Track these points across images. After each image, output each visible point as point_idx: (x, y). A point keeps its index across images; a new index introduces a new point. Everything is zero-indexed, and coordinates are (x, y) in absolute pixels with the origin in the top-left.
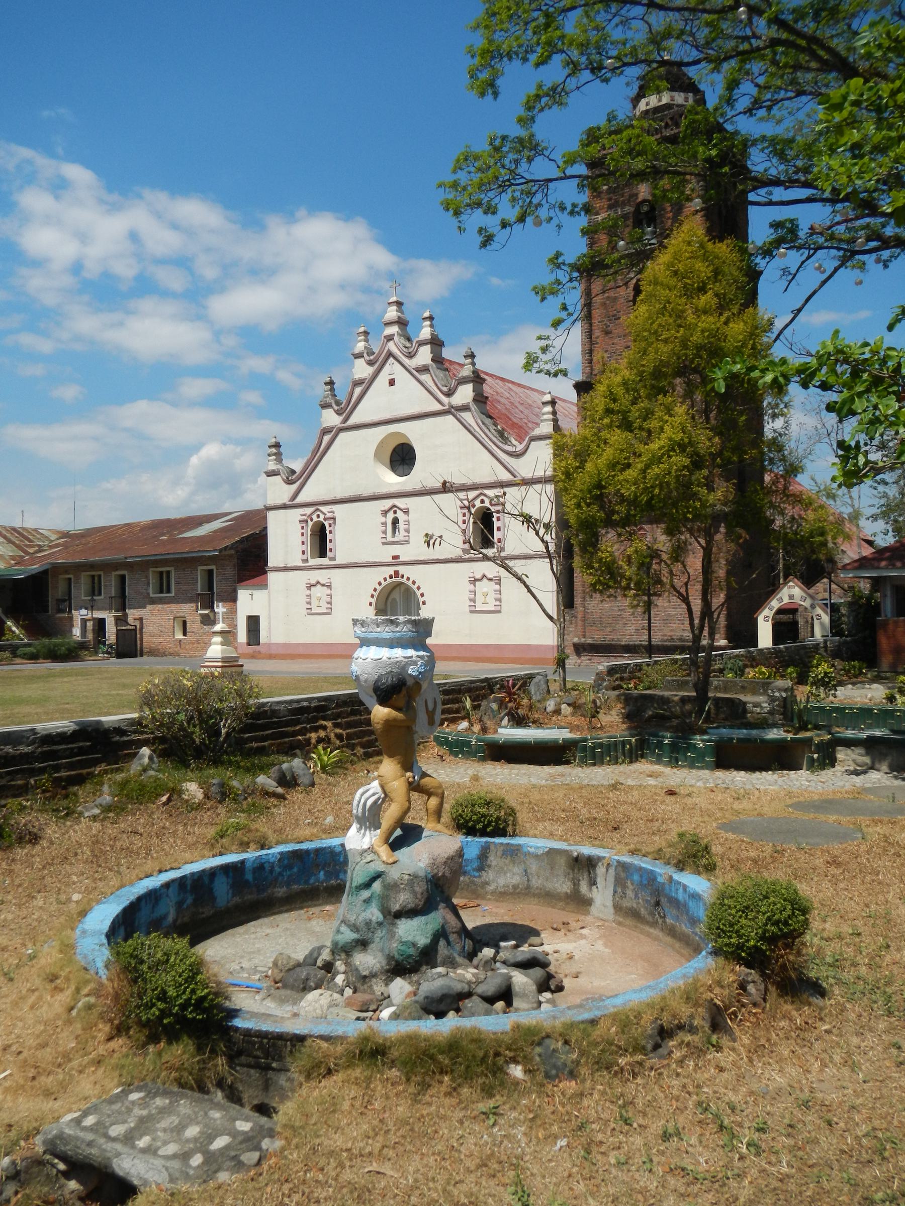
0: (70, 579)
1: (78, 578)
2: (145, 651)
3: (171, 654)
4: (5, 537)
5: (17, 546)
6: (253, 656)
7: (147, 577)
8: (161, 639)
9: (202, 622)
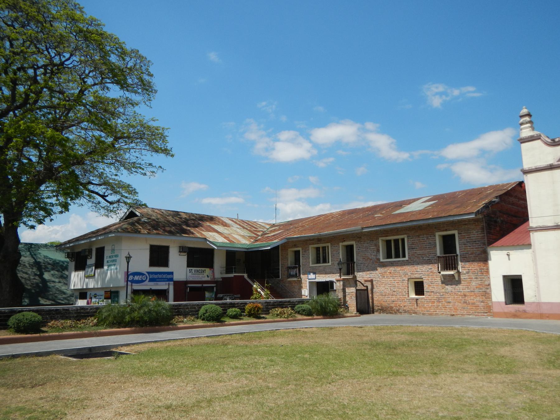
0: (299, 251)
1: (306, 250)
2: (376, 308)
3: (405, 312)
4: (240, 225)
5: (250, 231)
6: (515, 316)
7: (377, 246)
8: (394, 298)
9: (443, 283)
